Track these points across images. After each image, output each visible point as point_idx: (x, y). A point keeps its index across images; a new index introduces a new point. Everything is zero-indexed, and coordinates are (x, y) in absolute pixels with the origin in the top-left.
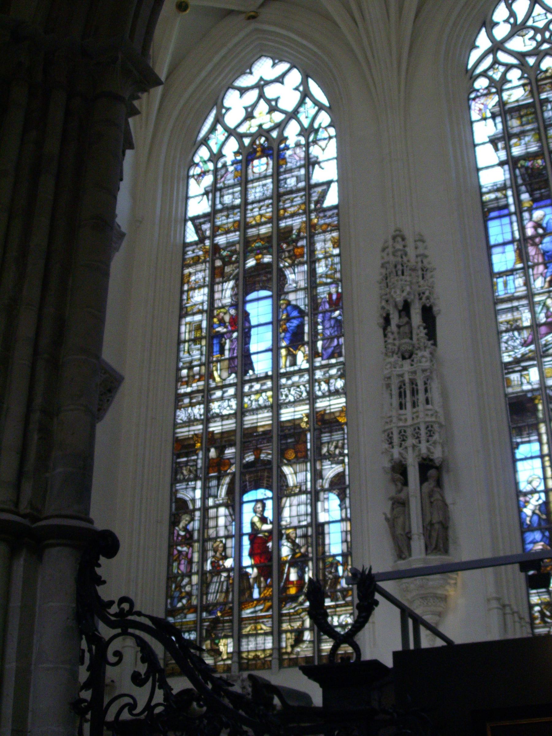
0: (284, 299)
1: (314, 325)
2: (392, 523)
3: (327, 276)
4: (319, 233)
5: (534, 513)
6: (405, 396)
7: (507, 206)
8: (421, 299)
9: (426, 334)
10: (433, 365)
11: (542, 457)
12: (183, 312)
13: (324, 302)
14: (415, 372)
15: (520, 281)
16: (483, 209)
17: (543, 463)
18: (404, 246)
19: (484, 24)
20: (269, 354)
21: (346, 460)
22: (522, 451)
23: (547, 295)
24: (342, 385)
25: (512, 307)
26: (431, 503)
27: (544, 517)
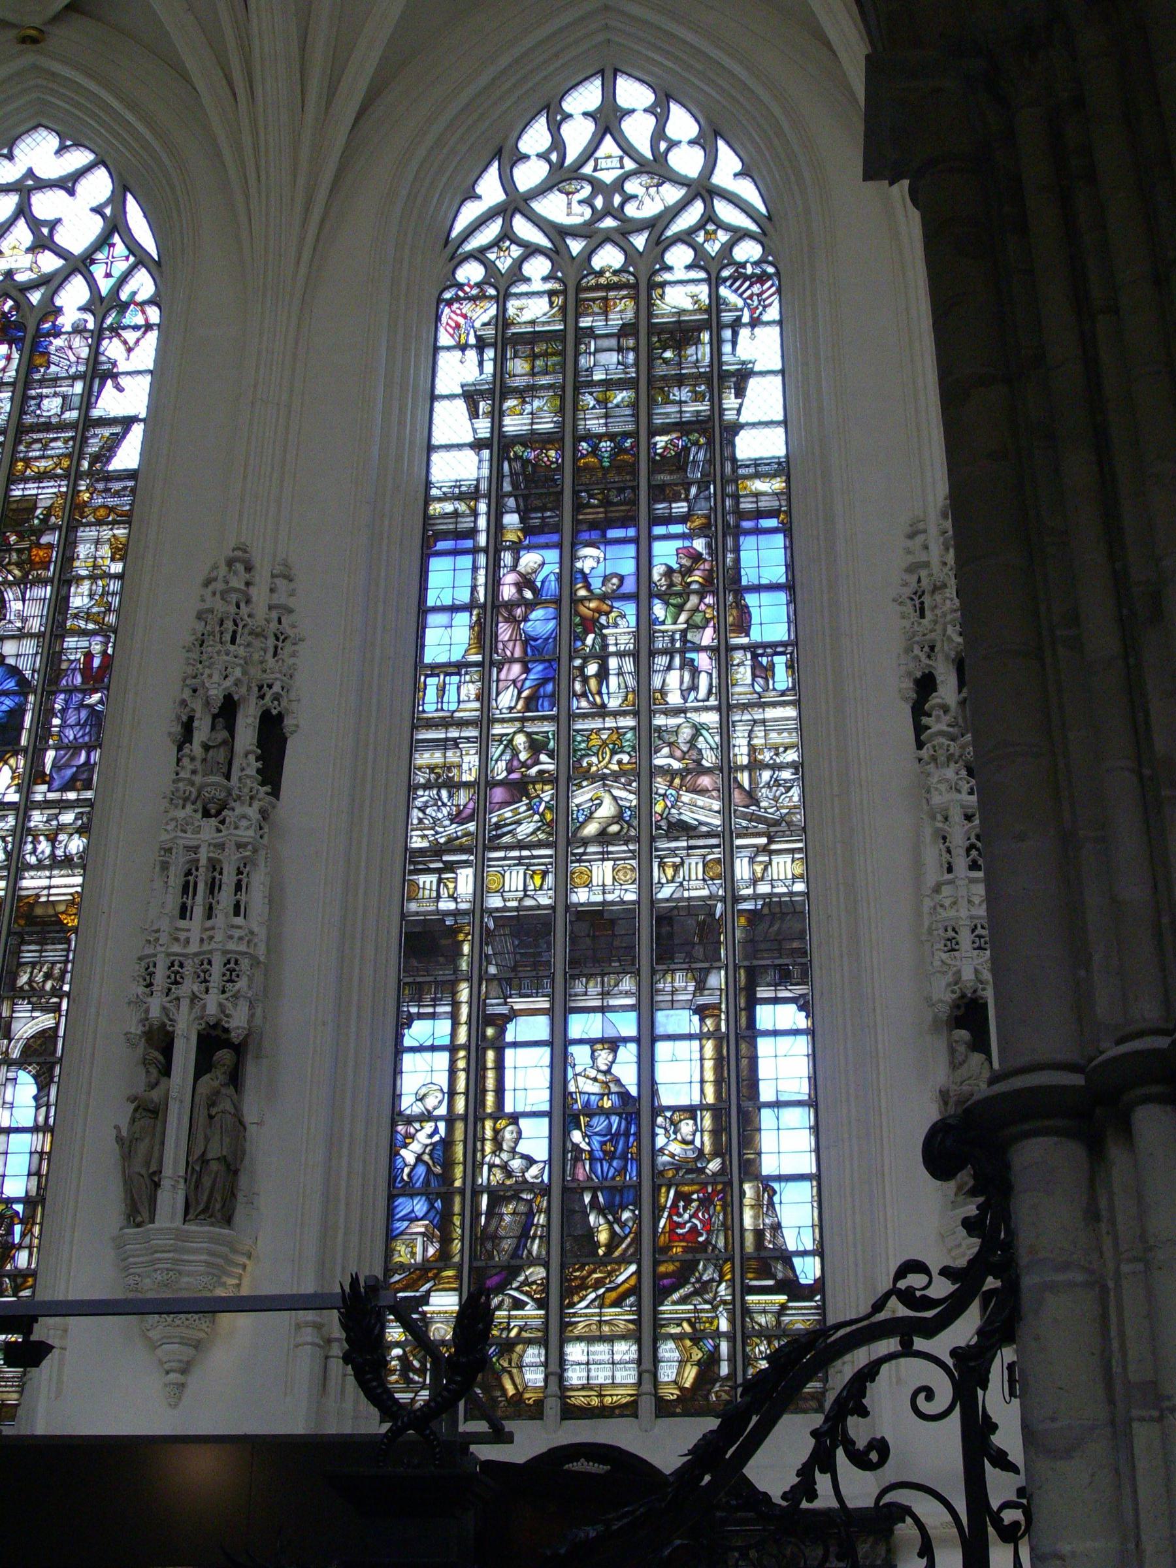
1: (45, 713)
2: (127, 1146)
3: (88, 617)
4: (89, 524)
5: (419, 1159)
6: (195, 894)
7: (472, 533)
8: (262, 697)
9: (258, 771)
10: (261, 837)
11: (452, 1049)
13: (74, 670)
14: (221, 846)
15: (470, 690)
16: (425, 530)
17: (453, 1062)
18: (248, 584)
19: (498, 154)
21: (64, 1006)
22: (418, 1032)
23: (518, 725)
24: (81, 849)
25: (447, 739)
26: (211, 1117)
27: (438, 1170)
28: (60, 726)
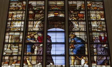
0: (72, 34)
12: (7, 30)
13: (97, 39)
20: (64, 58)
28: (96, 51)
